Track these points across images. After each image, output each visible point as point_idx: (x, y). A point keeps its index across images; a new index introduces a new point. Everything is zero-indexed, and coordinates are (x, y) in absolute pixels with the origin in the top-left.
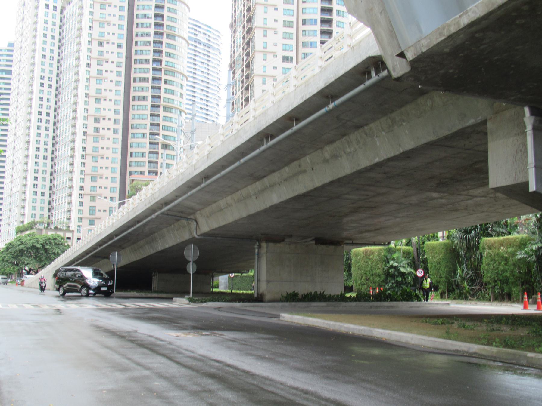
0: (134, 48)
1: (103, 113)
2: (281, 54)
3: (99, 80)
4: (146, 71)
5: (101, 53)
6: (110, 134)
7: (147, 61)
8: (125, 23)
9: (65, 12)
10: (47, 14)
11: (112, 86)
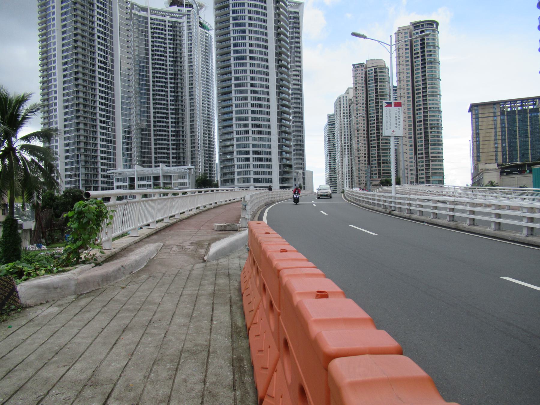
0: (370, 129)
1: (360, 155)
2: (408, 136)
3: (358, 144)
4: (374, 137)
5: (358, 134)
6: (363, 162)
7: (374, 133)
8: (365, 122)
9: (351, 107)
10: (344, 110)
11: (363, 145)
